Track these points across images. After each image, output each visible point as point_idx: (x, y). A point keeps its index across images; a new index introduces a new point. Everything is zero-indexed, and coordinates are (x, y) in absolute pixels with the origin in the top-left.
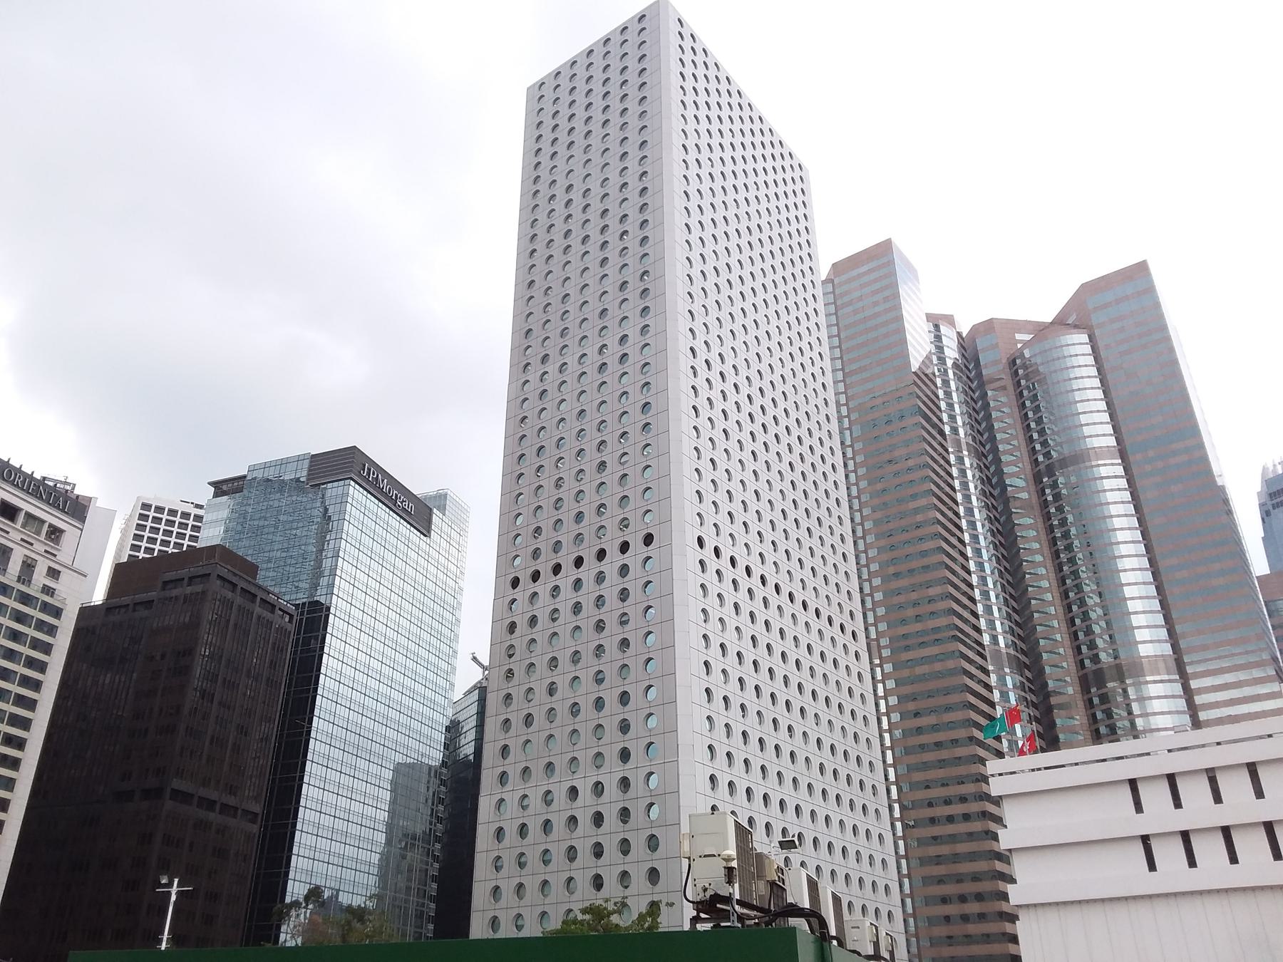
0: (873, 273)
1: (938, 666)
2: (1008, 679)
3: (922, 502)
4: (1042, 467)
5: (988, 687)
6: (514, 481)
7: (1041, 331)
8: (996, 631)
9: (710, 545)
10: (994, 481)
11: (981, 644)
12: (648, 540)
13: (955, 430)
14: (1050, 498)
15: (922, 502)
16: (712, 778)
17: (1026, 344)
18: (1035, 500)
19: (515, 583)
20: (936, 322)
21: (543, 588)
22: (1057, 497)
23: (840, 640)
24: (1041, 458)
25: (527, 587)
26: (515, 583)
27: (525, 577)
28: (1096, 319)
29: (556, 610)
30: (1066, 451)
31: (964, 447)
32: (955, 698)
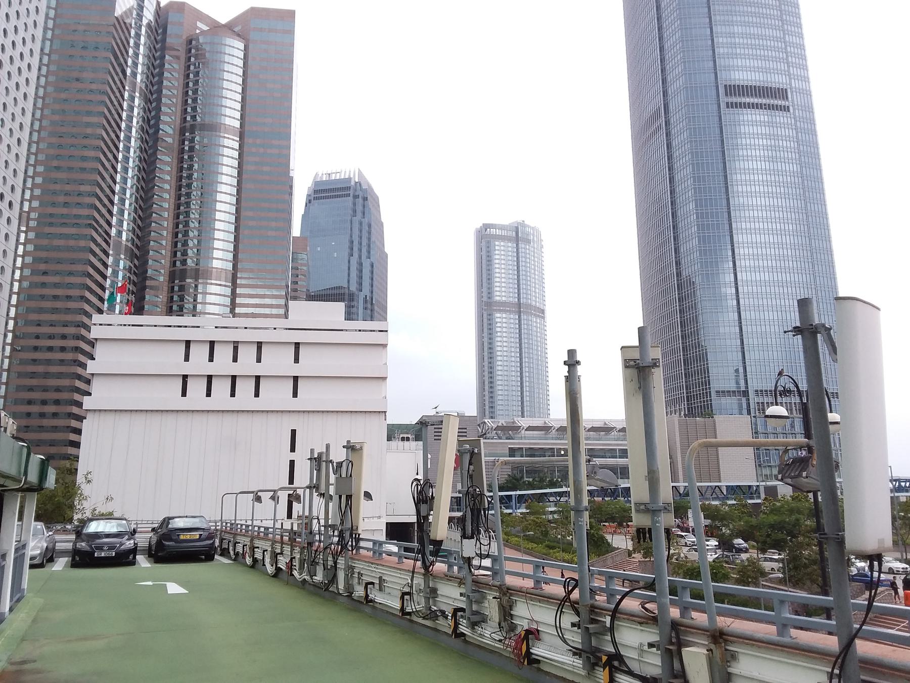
1: (72, 243)
2: (122, 263)
3: (94, 120)
5: (106, 265)
7: (216, 28)
8: (123, 229)
10: (152, 122)
13: (134, 74)
14: (187, 148)
15: (94, 120)
17: (203, 32)
18: (176, 146)
22: (192, 149)
24: (188, 118)
28: (253, 36)
30: (207, 120)
31: (138, 89)
32: (79, 268)
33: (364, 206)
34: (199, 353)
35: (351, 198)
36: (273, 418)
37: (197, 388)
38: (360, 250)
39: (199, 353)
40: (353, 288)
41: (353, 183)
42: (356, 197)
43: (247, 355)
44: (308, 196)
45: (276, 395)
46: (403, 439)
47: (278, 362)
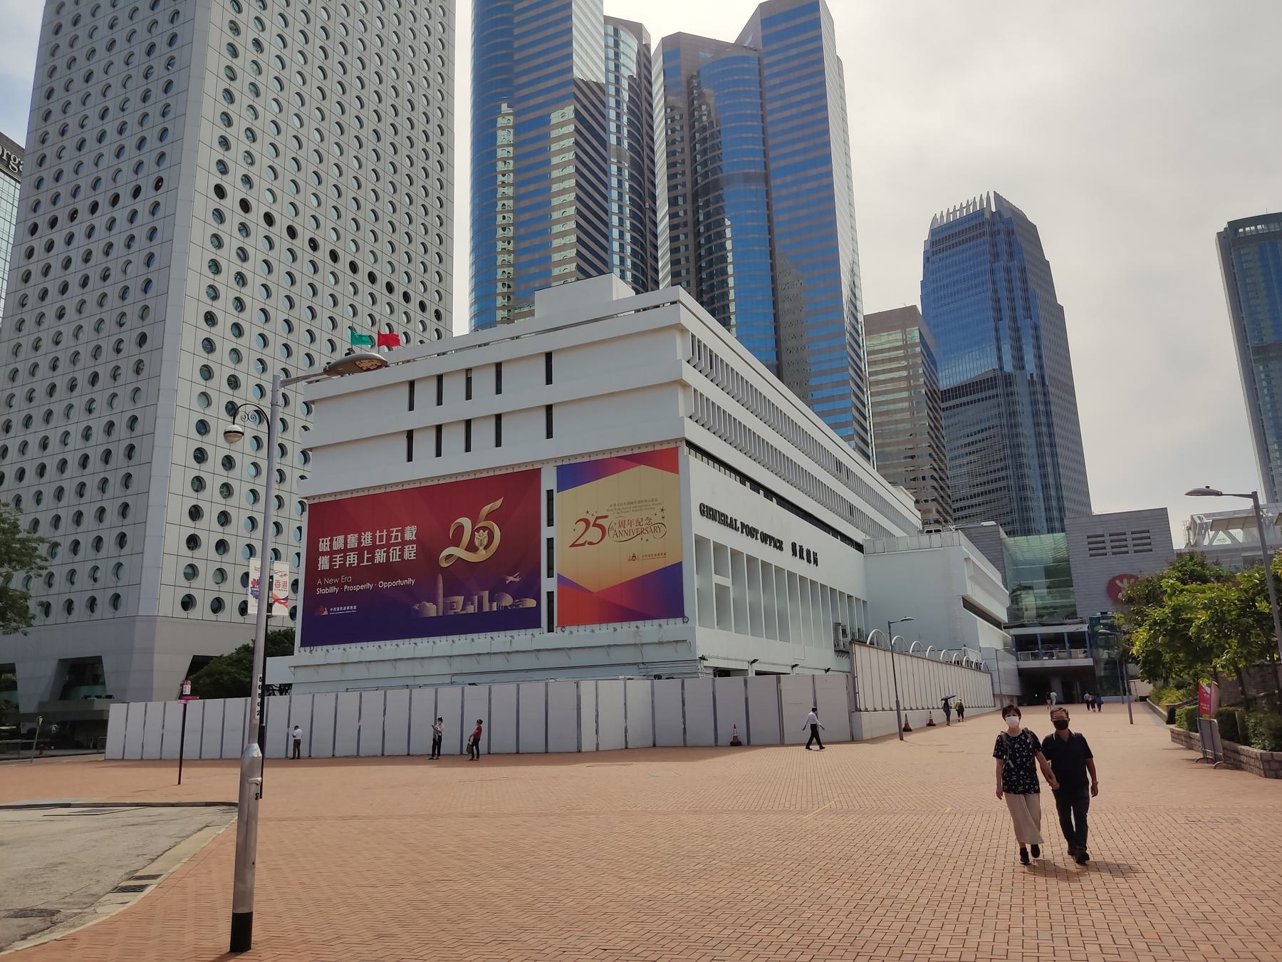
20: (617, 27)
25: (44, 234)
34: (426, 393)
35: (987, 238)
40: (1008, 368)
41: (987, 215)
43: (483, 383)
47: (525, 389)
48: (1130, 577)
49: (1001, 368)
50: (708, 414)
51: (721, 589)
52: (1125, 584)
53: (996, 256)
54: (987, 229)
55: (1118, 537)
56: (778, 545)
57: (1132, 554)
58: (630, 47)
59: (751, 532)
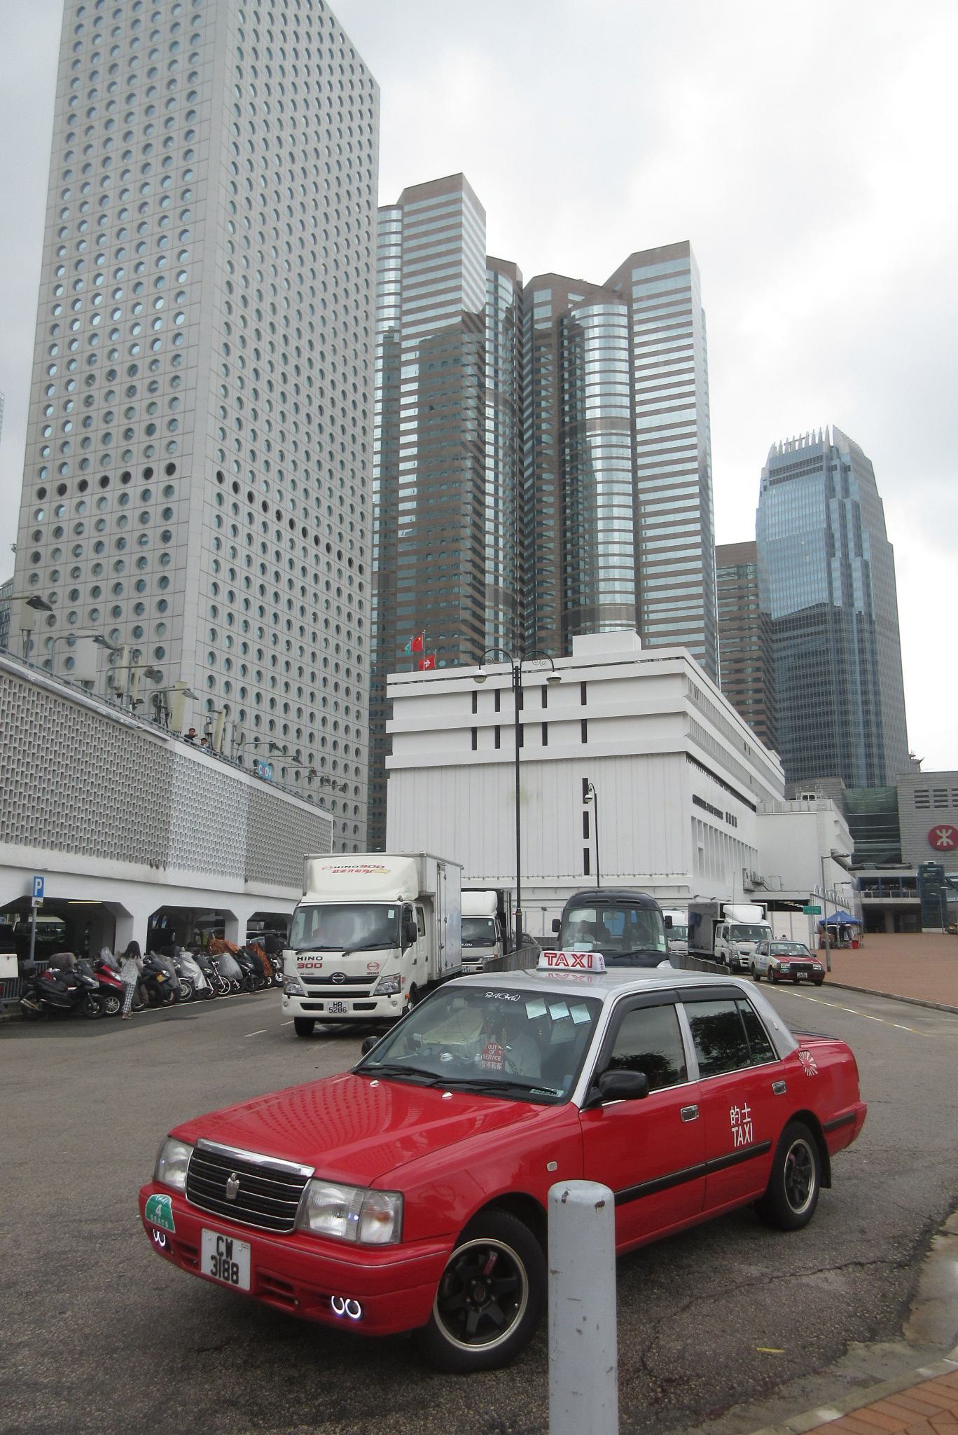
0: (441, 199)
4: (567, 428)
6: (43, 392)
9: (229, 480)
11: (483, 585)
12: (171, 469)
16: (211, 678)
18: (556, 459)
19: (42, 493)
21: (69, 501)
23: (347, 572)
25: (52, 498)
26: (42, 493)
27: (51, 489)
28: (637, 292)
29: (80, 524)
31: (500, 401)
33: (845, 480)
34: (486, 703)
36: (563, 768)
37: (486, 740)
38: (845, 545)
39: (486, 703)
40: (838, 603)
41: (825, 450)
42: (831, 469)
44: (763, 480)
45: (565, 742)
46: (805, 798)
47: (564, 705)
48: (947, 828)
49: (832, 603)
50: (697, 734)
51: (700, 850)
52: (944, 834)
53: (830, 491)
54: (824, 464)
55: (941, 794)
56: (718, 814)
57: (951, 808)
58: (506, 284)
59: (711, 809)
